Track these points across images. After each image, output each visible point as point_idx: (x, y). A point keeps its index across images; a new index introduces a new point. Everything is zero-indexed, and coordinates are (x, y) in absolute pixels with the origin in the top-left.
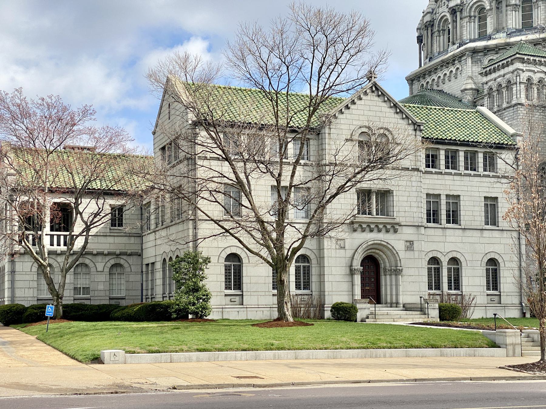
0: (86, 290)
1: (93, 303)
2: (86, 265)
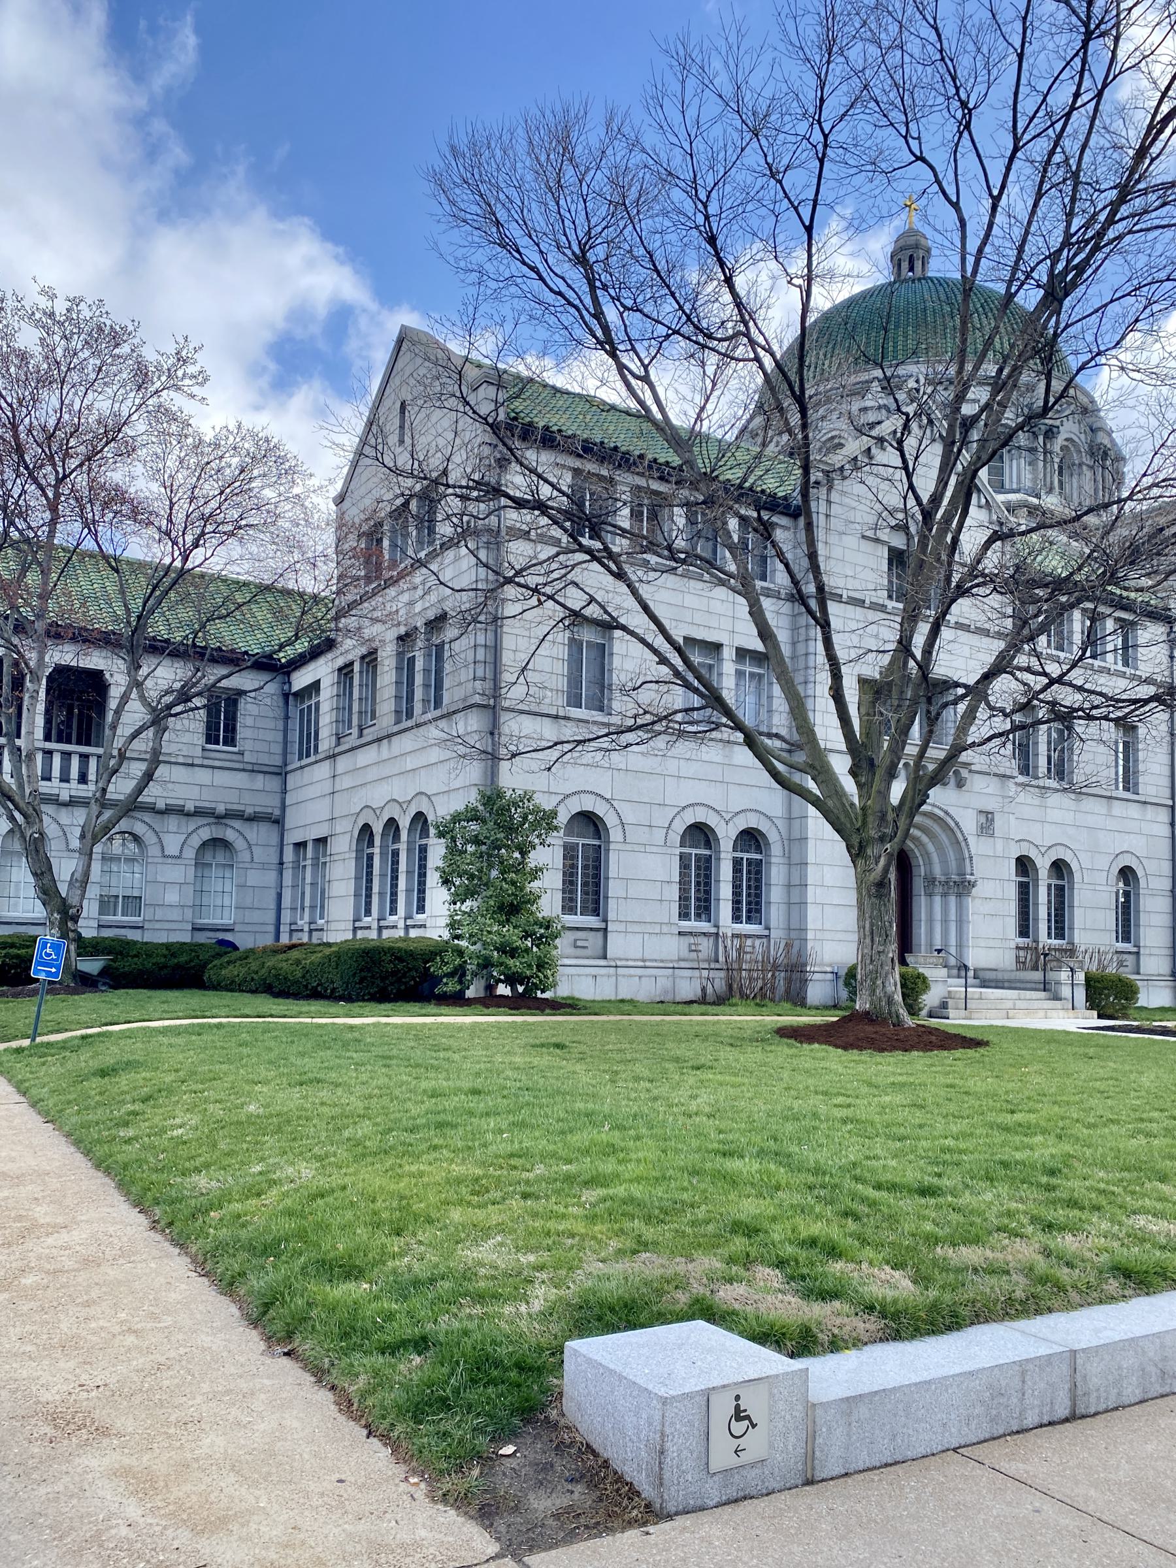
0: (133, 903)
1: (148, 937)
2: (136, 838)
